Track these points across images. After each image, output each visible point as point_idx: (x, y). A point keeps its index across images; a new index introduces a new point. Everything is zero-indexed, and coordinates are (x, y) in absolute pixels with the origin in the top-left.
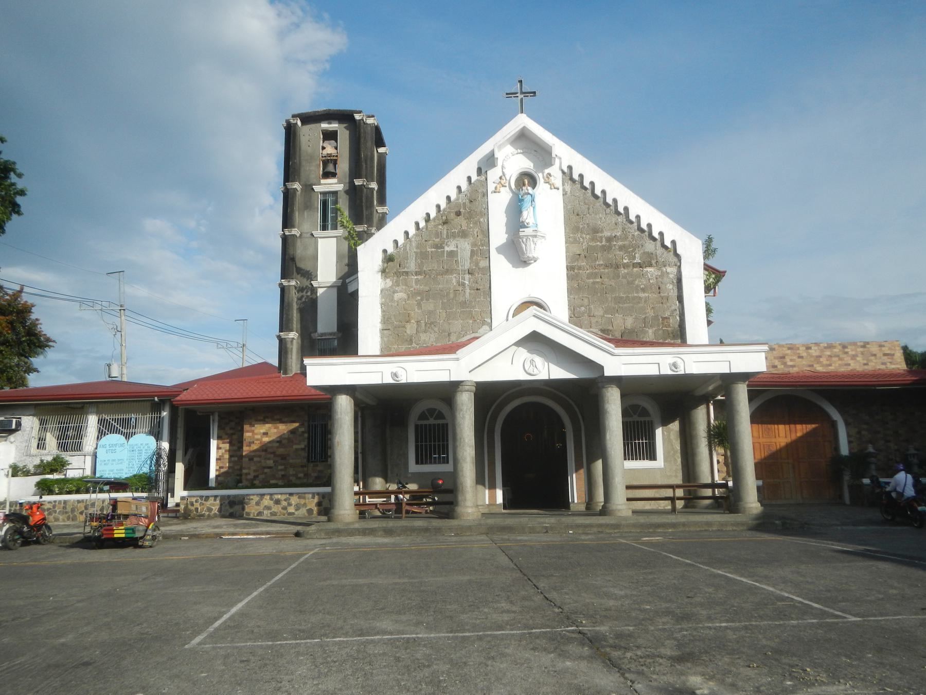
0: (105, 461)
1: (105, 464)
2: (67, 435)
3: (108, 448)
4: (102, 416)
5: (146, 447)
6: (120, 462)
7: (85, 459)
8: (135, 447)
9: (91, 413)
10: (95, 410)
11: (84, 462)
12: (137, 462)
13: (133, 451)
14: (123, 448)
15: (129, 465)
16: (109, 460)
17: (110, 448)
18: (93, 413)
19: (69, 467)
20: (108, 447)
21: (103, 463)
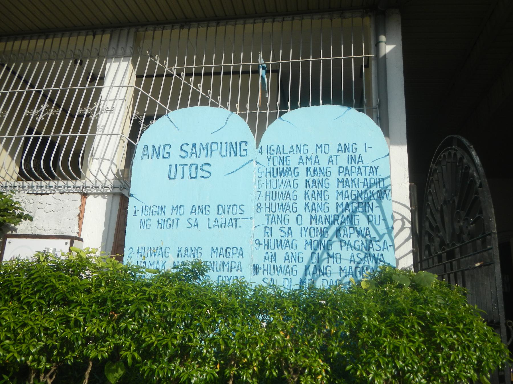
0: (162, 208)
1: (161, 224)
2: (28, 118)
3: (175, 158)
4: (153, 65)
5: (343, 160)
6: (228, 216)
7: (82, 208)
8: (294, 159)
9: (117, 56)
10: (131, 44)
11: (80, 217)
12: (306, 223)
13: (282, 173)
14: (240, 161)
15: (269, 231)
16: (178, 208)
17: (188, 161)
18: (125, 56)
19: (23, 227)
20: (175, 152)
21: (154, 220)
